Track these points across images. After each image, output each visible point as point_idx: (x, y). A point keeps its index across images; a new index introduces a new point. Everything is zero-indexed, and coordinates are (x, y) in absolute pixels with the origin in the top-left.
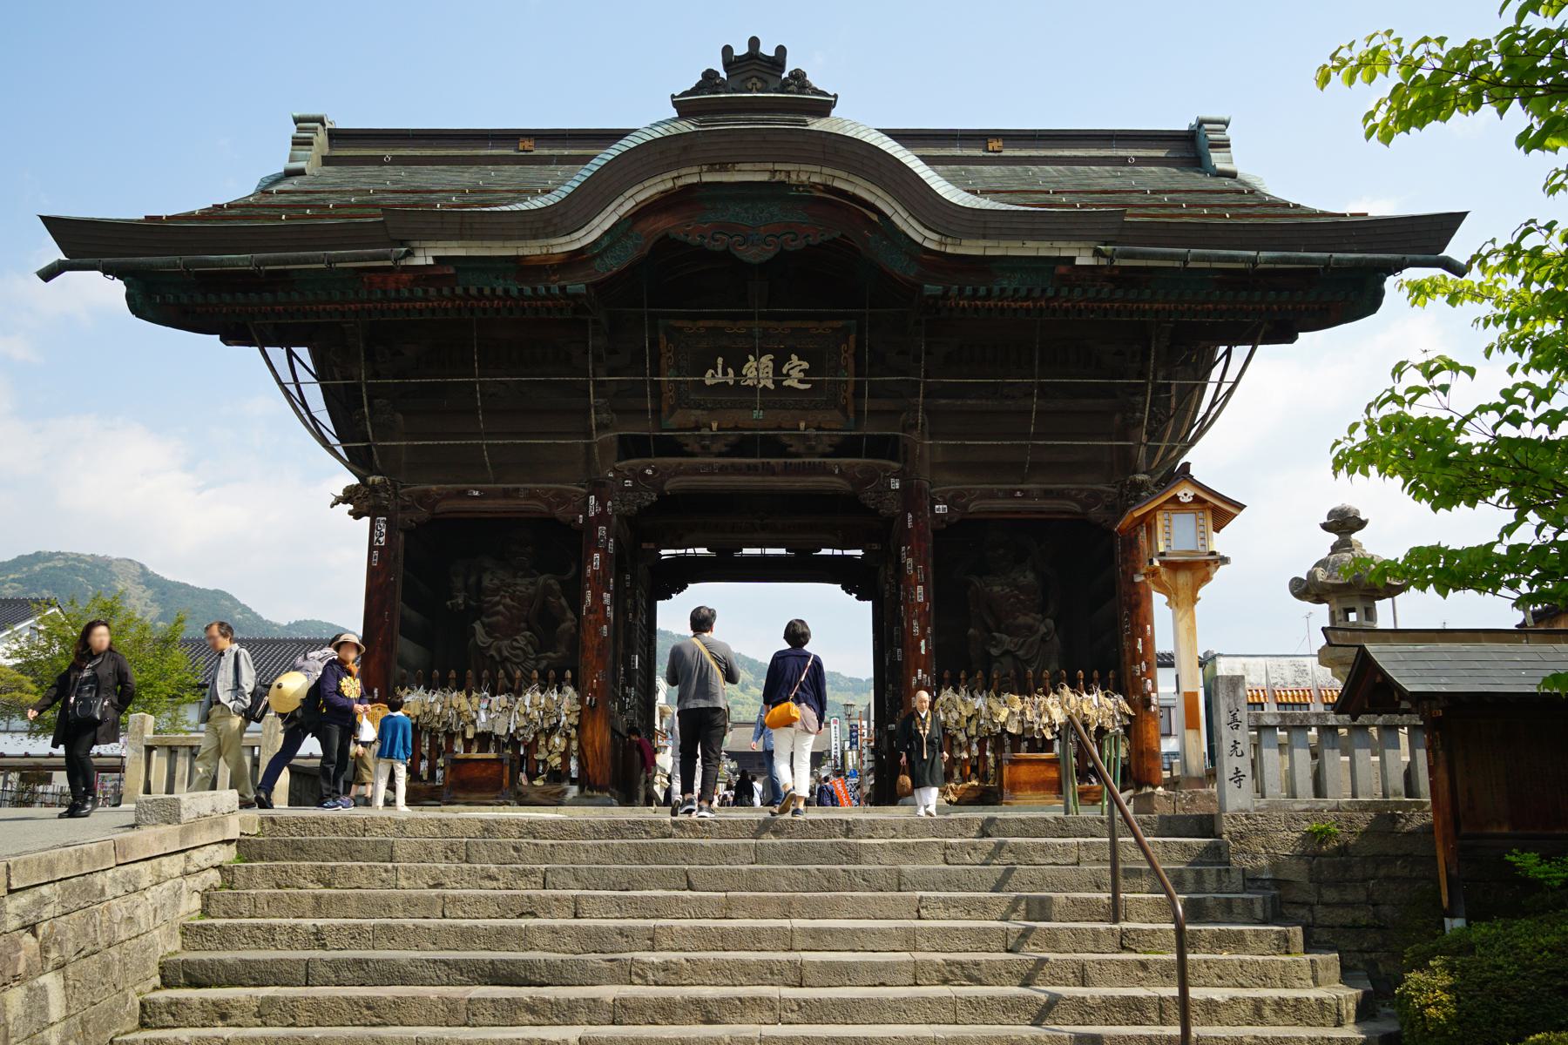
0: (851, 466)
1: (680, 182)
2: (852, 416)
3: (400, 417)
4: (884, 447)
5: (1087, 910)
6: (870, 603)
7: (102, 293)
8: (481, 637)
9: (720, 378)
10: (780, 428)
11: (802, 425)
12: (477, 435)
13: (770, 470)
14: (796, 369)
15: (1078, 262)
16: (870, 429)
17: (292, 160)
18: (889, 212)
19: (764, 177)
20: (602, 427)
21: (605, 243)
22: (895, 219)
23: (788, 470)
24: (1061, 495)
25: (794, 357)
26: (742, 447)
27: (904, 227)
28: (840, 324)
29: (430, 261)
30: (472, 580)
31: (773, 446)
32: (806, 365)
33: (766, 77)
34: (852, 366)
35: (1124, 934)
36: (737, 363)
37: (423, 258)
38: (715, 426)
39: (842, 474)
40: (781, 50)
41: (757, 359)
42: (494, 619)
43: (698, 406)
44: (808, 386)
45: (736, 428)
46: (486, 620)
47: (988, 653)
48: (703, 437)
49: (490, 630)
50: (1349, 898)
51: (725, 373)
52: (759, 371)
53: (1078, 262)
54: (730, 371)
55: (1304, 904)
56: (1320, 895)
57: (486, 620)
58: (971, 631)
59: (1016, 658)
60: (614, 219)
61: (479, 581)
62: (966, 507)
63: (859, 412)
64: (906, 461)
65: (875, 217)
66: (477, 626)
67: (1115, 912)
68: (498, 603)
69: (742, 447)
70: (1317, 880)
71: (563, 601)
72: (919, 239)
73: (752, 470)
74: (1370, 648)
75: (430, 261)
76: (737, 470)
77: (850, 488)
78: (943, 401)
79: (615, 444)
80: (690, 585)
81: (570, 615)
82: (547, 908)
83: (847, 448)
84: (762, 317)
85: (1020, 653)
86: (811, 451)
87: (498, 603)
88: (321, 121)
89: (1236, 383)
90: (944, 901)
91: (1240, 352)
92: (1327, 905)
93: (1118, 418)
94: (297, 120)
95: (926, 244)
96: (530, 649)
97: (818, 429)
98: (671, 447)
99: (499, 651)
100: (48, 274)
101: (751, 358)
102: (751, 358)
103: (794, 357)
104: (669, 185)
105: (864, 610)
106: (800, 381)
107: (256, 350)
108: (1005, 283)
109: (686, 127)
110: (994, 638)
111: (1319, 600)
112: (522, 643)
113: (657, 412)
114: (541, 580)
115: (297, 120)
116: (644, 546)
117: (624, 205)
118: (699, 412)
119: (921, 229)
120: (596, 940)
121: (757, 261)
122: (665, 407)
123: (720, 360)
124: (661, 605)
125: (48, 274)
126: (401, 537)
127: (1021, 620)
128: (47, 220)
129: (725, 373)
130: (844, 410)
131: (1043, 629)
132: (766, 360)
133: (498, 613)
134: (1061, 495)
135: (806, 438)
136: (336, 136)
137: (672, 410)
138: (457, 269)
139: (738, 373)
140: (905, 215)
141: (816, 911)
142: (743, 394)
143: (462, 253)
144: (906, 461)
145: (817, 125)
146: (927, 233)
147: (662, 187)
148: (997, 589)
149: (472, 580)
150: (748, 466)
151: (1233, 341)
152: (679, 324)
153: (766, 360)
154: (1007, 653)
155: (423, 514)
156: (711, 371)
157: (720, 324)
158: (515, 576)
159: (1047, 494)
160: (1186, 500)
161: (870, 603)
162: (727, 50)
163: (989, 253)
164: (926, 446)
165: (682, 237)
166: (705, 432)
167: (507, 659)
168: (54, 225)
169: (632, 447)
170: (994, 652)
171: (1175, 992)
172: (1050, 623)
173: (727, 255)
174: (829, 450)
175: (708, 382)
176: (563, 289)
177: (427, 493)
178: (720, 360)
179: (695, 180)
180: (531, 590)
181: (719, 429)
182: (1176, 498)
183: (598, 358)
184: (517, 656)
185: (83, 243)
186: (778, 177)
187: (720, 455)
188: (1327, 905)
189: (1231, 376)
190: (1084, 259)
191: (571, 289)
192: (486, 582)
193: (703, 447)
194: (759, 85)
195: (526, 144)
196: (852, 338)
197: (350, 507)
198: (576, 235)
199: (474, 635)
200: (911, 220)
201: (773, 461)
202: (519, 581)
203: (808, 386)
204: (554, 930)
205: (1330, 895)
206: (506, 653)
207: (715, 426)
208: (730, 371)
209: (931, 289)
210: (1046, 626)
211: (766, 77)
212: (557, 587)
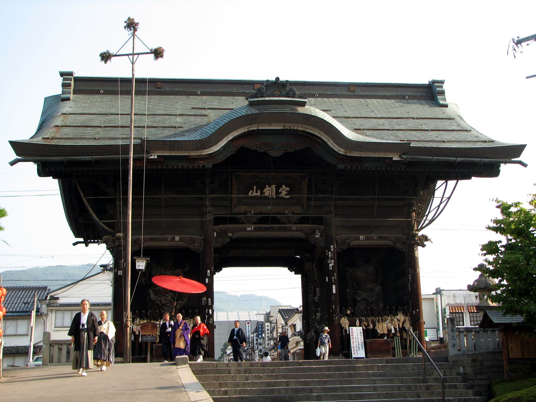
1: (251, 129)
4: (318, 221)
5: (418, 381)
6: (300, 276)
8: (153, 296)
11: (287, 212)
13: (273, 229)
14: (284, 191)
15: (394, 159)
17: (63, 93)
18: (326, 140)
19: (281, 128)
21: (221, 150)
22: (329, 143)
23: (281, 229)
24: (385, 238)
25: (284, 186)
26: (263, 220)
27: (332, 146)
28: (302, 174)
29: (156, 157)
31: (275, 220)
32: (288, 189)
33: (281, 90)
34: (306, 190)
35: (427, 386)
36: (261, 188)
37: (154, 157)
38: (253, 212)
39: (302, 231)
41: (269, 187)
43: (246, 204)
45: (261, 213)
47: (356, 299)
48: (248, 217)
51: (257, 192)
52: (269, 191)
53: (394, 159)
54: (259, 191)
55: (471, 380)
58: (348, 290)
59: (367, 301)
60: (226, 142)
62: (349, 243)
65: (320, 142)
67: (425, 381)
69: (263, 220)
70: (475, 373)
72: (337, 151)
73: (267, 229)
74: (487, 311)
75: (156, 157)
76: (261, 229)
78: (340, 202)
79: (213, 219)
80: (224, 269)
83: (303, 220)
84: (273, 172)
85: (369, 299)
86: (289, 222)
88: (71, 74)
89: (449, 198)
91: (451, 183)
92: (478, 379)
93: (406, 208)
94: (62, 74)
95: (340, 152)
97: (293, 213)
98: (234, 220)
99: (161, 301)
100: (13, 163)
101: (267, 186)
102: (267, 186)
103: (284, 186)
104: (246, 130)
105: (298, 278)
108: (367, 165)
109: (254, 111)
111: (475, 291)
112: (170, 298)
113: (231, 206)
115: (62, 74)
117: (230, 137)
118: (246, 207)
119: (338, 147)
121: (277, 156)
123: (255, 187)
125: (13, 163)
127: (369, 286)
129: (257, 192)
131: (377, 290)
134: (385, 238)
135: (289, 217)
136: (78, 80)
138: (164, 159)
140: (332, 142)
141: (350, 382)
142: (264, 200)
143: (169, 154)
145: (301, 110)
146: (340, 149)
147: (243, 131)
150: (265, 228)
151: (447, 178)
152: (240, 174)
154: (363, 299)
159: (380, 238)
161: (300, 276)
164: (335, 220)
165: (249, 147)
167: (164, 305)
169: (218, 221)
170: (358, 299)
172: (379, 287)
173: (265, 154)
174: (297, 221)
176: (204, 166)
178: (255, 187)
179: (256, 128)
181: (254, 214)
184: (168, 303)
186: (286, 128)
188: (478, 379)
189: (447, 195)
190: (396, 158)
191: (207, 166)
193: (248, 221)
194: (279, 93)
195: (159, 85)
196: (307, 179)
198: (212, 148)
200: (334, 144)
201: (275, 226)
204: (286, 389)
205: (478, 377)
206: (163, 302)
207: (253, 212)
208: (259, 191)
209: (341, 167)
210: (378, 289)
211: (281, 90)
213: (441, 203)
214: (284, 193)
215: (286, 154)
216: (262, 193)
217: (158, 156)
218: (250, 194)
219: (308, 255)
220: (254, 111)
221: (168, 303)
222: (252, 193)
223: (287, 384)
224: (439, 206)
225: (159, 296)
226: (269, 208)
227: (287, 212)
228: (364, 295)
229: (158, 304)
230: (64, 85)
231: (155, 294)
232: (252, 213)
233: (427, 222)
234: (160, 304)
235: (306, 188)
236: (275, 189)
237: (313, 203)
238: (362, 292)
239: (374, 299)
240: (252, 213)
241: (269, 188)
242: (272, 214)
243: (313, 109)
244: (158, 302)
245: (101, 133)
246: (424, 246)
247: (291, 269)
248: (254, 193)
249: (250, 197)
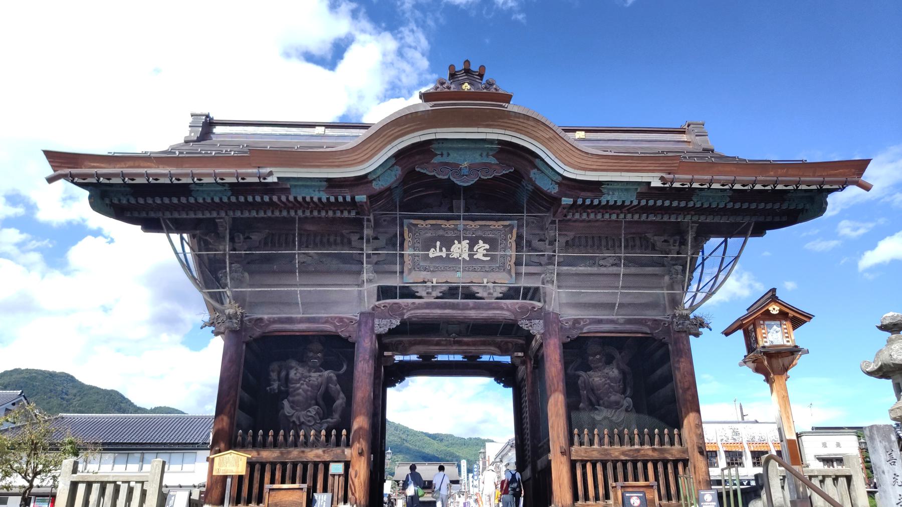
0: (514, 304)
2: (514, 275)
3: (246, 275)
9: (438, 254)
10: (472, 282)
11: (485, 281)
12: (296, 285)
13: (466, 307)
14: (481, 248)
15: (652, 185)
16: (523, 283)
20: (370, 281)
21: (379, 172)
25: (481, 242)
28: (507, 223)
30: (283, 374)
32: (487, 246)
36: (448, 244)
38: (434, 281)
39: (508, 310)
40: (482, 68)
41: (460, 242)
42: (297, 398)
43: (425, 270)
44: (488, 258)
45: (447, 282)
46: (291, 399)
47: (594, 419)
49: (293, 405)
51: (441, 250)
52: (460, 250)
53: (652, 185)
54: (444, 249)
57: (291, 399)
59: (611, 421)
61: (287, 375)
63: (518, 274)
64: (545, 302)
66: (285, 402)
68: (299, 388)
69: (452, 292)
71: (338, 386)
77: (513, 317)
79: (376, 291)
81: (342, 395)
85: (614, 418)
87: (299, 388)
91: (734, 242)
94: (192, 116)
96: (317, 417)
97: (494, 283)
99: (299, 418)
103: (481, 242)
105: (510, 391)
106: (484, 255)
107: (163, 236)
108: (609, 198)
109: (428, 106)
113: (402, 272)
114: (326, 373)
116: (386, 353)
122: (406, 269)
123: (438, 243)
124: (390, 391)
126: (244, 347)
127: (614, 398)
129: (441, 250)
130: (509, 272)
133: (299, 394)
137: (410, 271)
139: (448, 249)
142: (450, 262)
144: (545, 302)
148: (596, 379)
149: (283, 374)
153: (465, 243)
155: (258, 332)
156: (433, 249)
157: (439, 222)
158: (309, 371)
160: (775, 312)
162: (452, 67)
163: (601, 179)
166: (429, 284)
167: (303, 423)
172: (629, 399)
175: (431, 255)
176: (353, 198)
177: (261, 320)
178: (438, 243)
180: (320, 379)
182: (768, 311)
183: (368, 241)
184: (309, 421)
187: (437, 298)
192: (292, 374)
197: (213, 328)
199: (283, 408)
202: (313, 374)
203: (488, 258)
206: (302, 420)
208: (444, 249)
212: (335, 378)
213: (720, 271)
215: (480, 183)
217: (278, 178)
219: (520, 354)
220: (428, 106)
221: (309, 421)
224: (717, 277)
225: (297, 410)
226: (459, 274)
227: (485, 281)
229: (294, 422)
231: (292, 407)
233: (700, 296)
234: (298, 423)
235: (514, 245)
236: (467, 246)
237: (524, 269)
241: (459, 246)
244: (294, 419)
246: (697, 335)
247: (498, 380)
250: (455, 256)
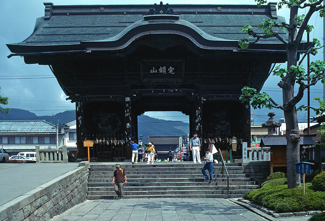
7: (20, 59)
9: (154, 72)
17: (45, 15)
36: (158, 68)
41: (162, 68)
45: (158, 83)
50: (261, 174)
51: (155, 71)
52: (162, 70)
54: (156, 70)
56: (256, 174)
82: (139, 177)
88: (51, 4)
90: (198, 175)
94: (45, 4)
100: (9, 57)
109: (147, 23)
110: (216, 126)
115: (45, 4)
117: (133, 39)
120: (147, 181)
123: (154, 68)
125: (9, 57)
127: (223, 122)
128: (8, 46)
129: (155, 71)
131: (227, 124)
132: (164, 67)
154: (219, 129)
168: (9, 46)
170: (216, 129)
171: (229, 186)
178: (154, 68)
185: (15, 49)
198: (123, 46)
205: (258, 174)
208: (156, 70)
214: (171, 71)
216: (158, 71)
218: (151, 72)
222: (152, 71)
223: (143, 177)
228: (219, 127)
230: (46, 11)
232: (153, 83)
238: (219, 126)
239: (225, 129)
240: (153, 83)
241: (162, 68)
242: (164, 83)
243: (183, 21)
245: (62, 38)
248: (153, 71)
249: (152, 73)
250: (161, 72)
